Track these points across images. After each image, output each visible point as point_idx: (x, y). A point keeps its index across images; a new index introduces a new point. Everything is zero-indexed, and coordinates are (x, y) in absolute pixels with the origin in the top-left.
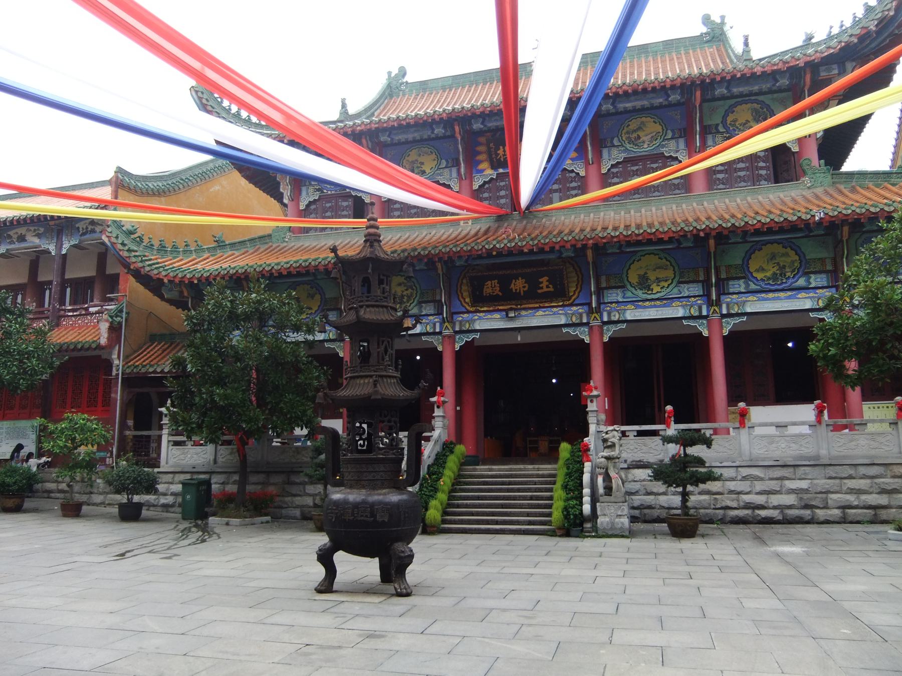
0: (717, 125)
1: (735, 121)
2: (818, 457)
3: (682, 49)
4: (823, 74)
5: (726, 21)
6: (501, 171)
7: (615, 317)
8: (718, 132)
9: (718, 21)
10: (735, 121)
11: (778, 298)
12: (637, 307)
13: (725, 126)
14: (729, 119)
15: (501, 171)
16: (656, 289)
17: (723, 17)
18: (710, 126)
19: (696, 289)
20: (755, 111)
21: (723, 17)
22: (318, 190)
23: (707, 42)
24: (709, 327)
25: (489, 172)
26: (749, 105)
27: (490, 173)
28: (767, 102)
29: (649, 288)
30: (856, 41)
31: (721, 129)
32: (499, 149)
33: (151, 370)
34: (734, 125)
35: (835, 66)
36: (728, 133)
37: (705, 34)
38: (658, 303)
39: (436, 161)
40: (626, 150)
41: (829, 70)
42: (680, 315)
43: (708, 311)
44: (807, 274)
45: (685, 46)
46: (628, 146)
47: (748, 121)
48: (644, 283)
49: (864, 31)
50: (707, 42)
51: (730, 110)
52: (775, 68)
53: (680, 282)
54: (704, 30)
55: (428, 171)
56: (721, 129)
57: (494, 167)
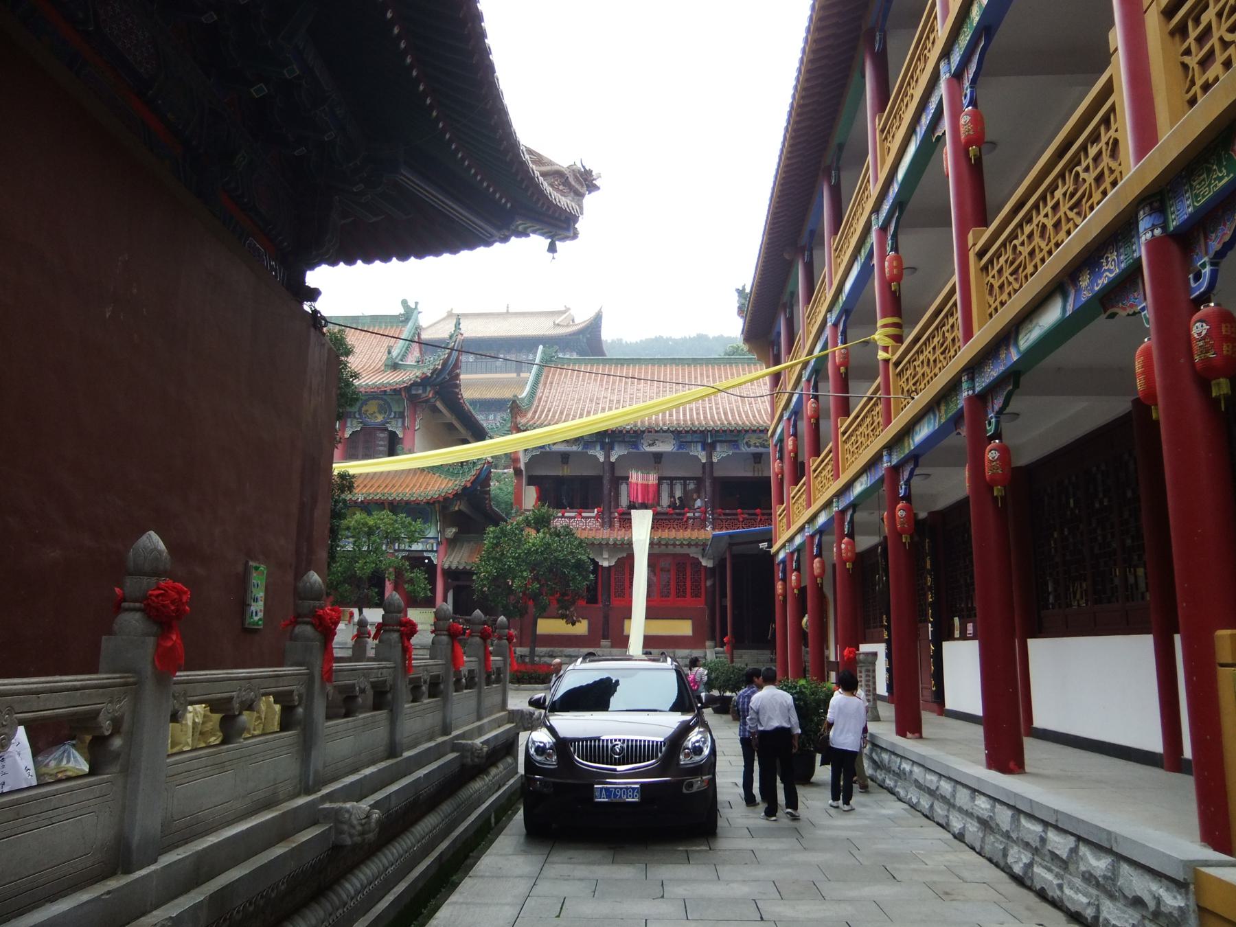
0: (355, 412)
1: (367, 411)
2: (346, 643)
3: (383, 325)
4: (414, 392)
5: (419, 307)
8: (355, 418)
9: (413, 306)
10: (367, 411)
13: (360, 414)
14: (363, 409)
17: (416, 303)
18: (350, 412)
20: (380, 406)
21: (416, 303)
23: (402, 322)
26: (377, 401)
28: (389, 400)
30: (419, 381)
31: (357, 416)
34: (366, 414)
35: (421, 388)
36: (361, 419)
37: (402, 315)
41: (417, 390)
45: (386, 323)
47: (374, 412)
49: (424, 376)
50: (402, 322)
51: (365, 403)
52: (373, 390)
54: (402, 311)
56: (357, 416)
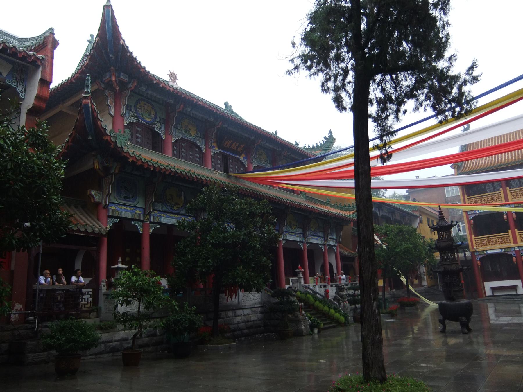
6: (221, 150)
7: (285, 238)
11: (314, 239)
12: (289, 235)
15: (221, 150)
16: (293, 229)
19: (300, 231)
22: (136, 117)
24: (304, 246)
25: (216, 149)
27: (217, 150)
29: (292, 228)
32: (227, 141)
33: (75, 228)
38: (293, 234)
39: (196, 132)
40: (258, 162)
42: (298, 240)
43: (304, 240)
44: (320, 231)
46: (259, 160)
48: (291, 226)
53: (299, 228)
55: (193, 135)
57: (219, 148)
